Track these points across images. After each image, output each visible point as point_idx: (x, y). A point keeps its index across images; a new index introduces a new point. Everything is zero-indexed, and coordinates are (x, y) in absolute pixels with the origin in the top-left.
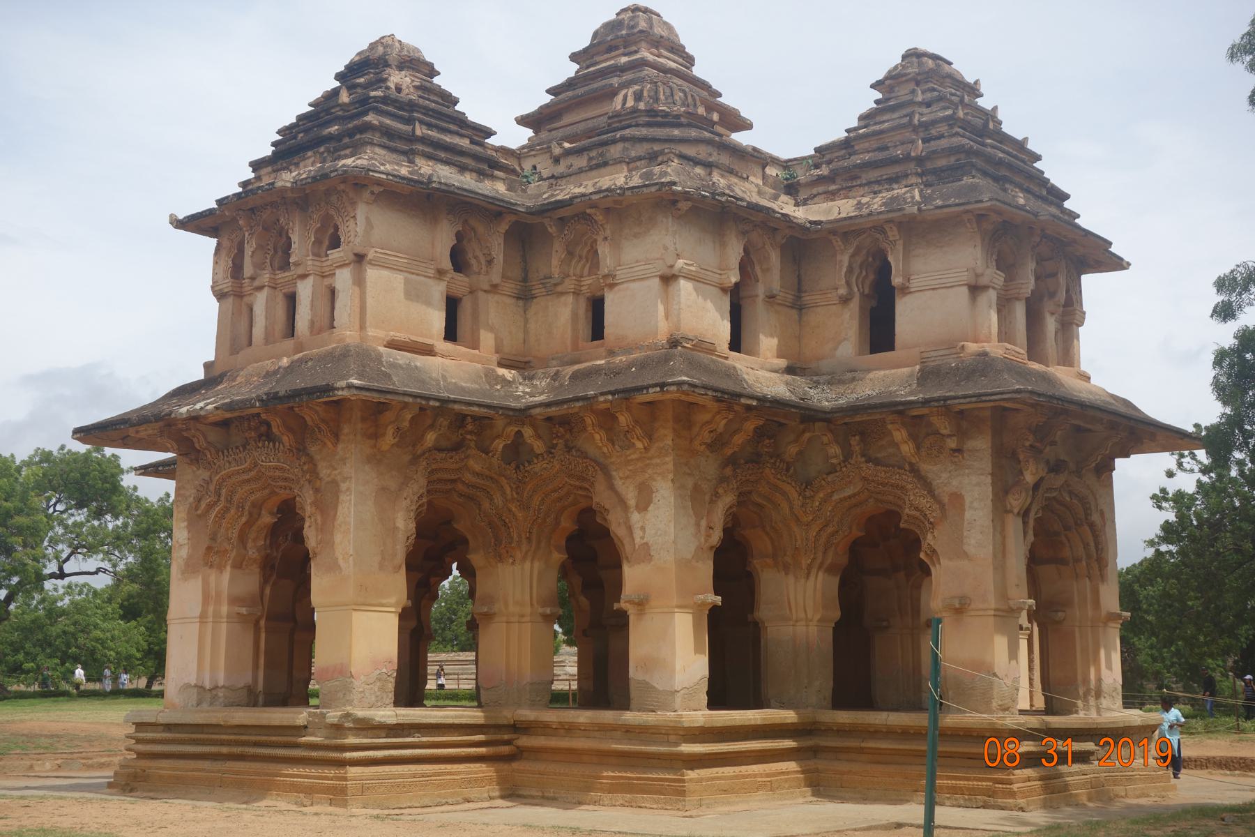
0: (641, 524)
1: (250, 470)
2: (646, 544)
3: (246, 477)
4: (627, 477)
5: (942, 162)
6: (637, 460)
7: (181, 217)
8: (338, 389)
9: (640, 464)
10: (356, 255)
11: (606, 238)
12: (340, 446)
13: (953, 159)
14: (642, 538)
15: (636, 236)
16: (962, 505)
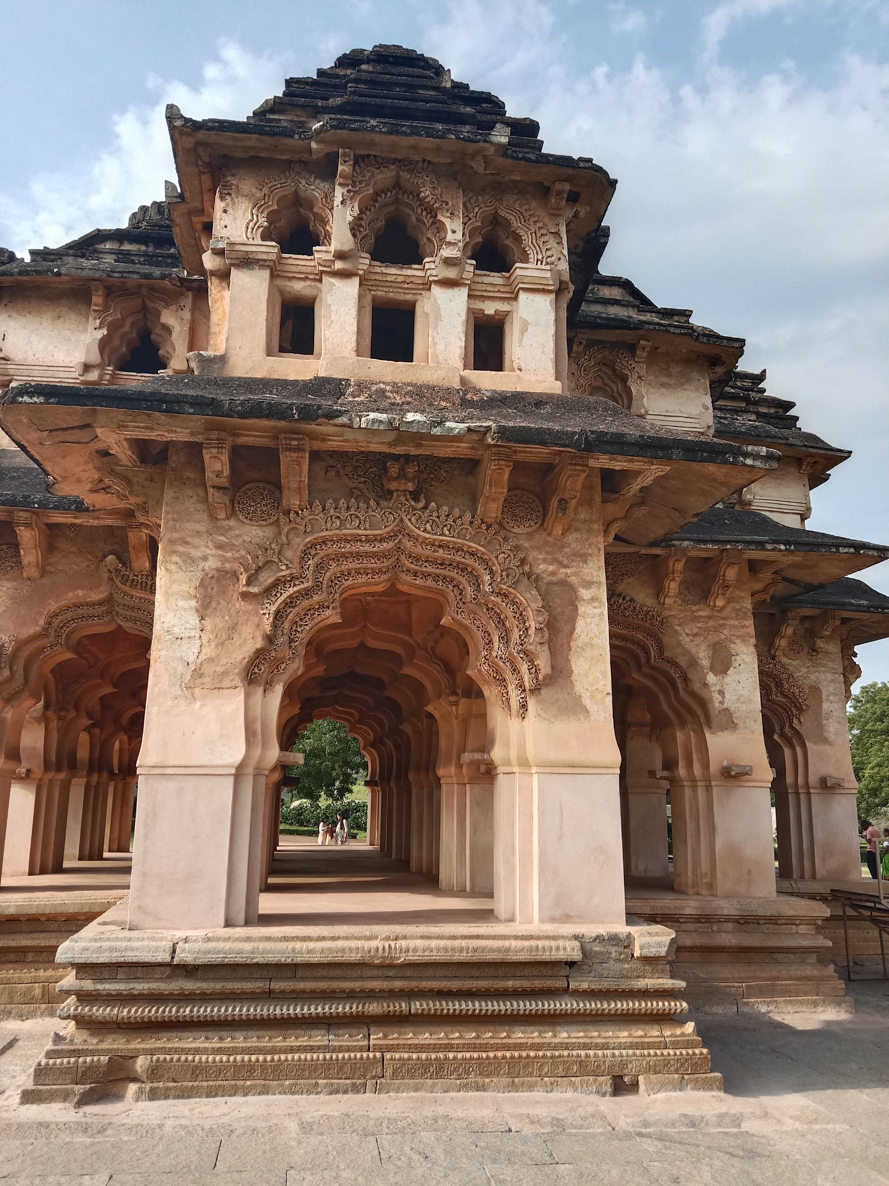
0: (718, 688)
1: (381, 541)
2: (727, 710)
3: (367, 548)
4: (696, 635)
5: (765, 410)
6: (710, 617)
7: (198, 118)
8: (746, 455)
9: (711, 623)
10: (561, 282)
11: (640, 377)
12: (571, 537)
13: (772, 411)
14: (722, 703)
15: (663, 385)
16: (820, 697)
